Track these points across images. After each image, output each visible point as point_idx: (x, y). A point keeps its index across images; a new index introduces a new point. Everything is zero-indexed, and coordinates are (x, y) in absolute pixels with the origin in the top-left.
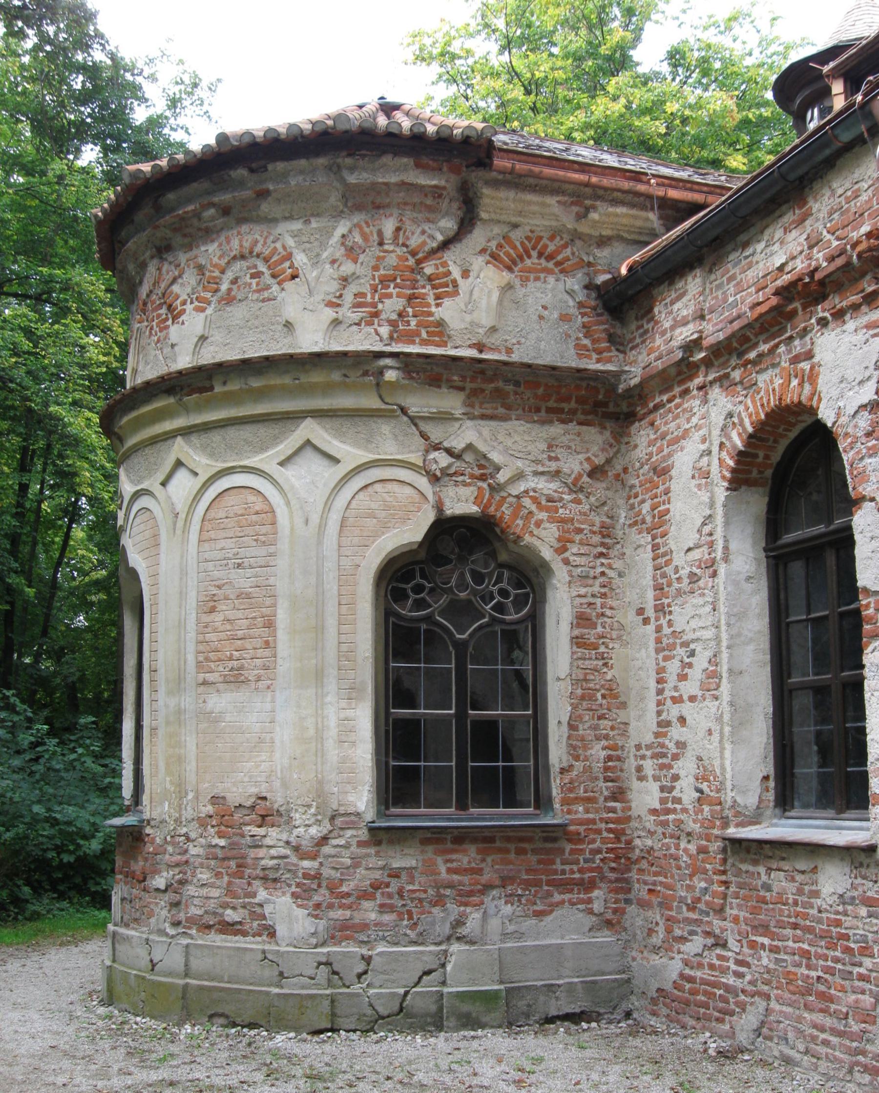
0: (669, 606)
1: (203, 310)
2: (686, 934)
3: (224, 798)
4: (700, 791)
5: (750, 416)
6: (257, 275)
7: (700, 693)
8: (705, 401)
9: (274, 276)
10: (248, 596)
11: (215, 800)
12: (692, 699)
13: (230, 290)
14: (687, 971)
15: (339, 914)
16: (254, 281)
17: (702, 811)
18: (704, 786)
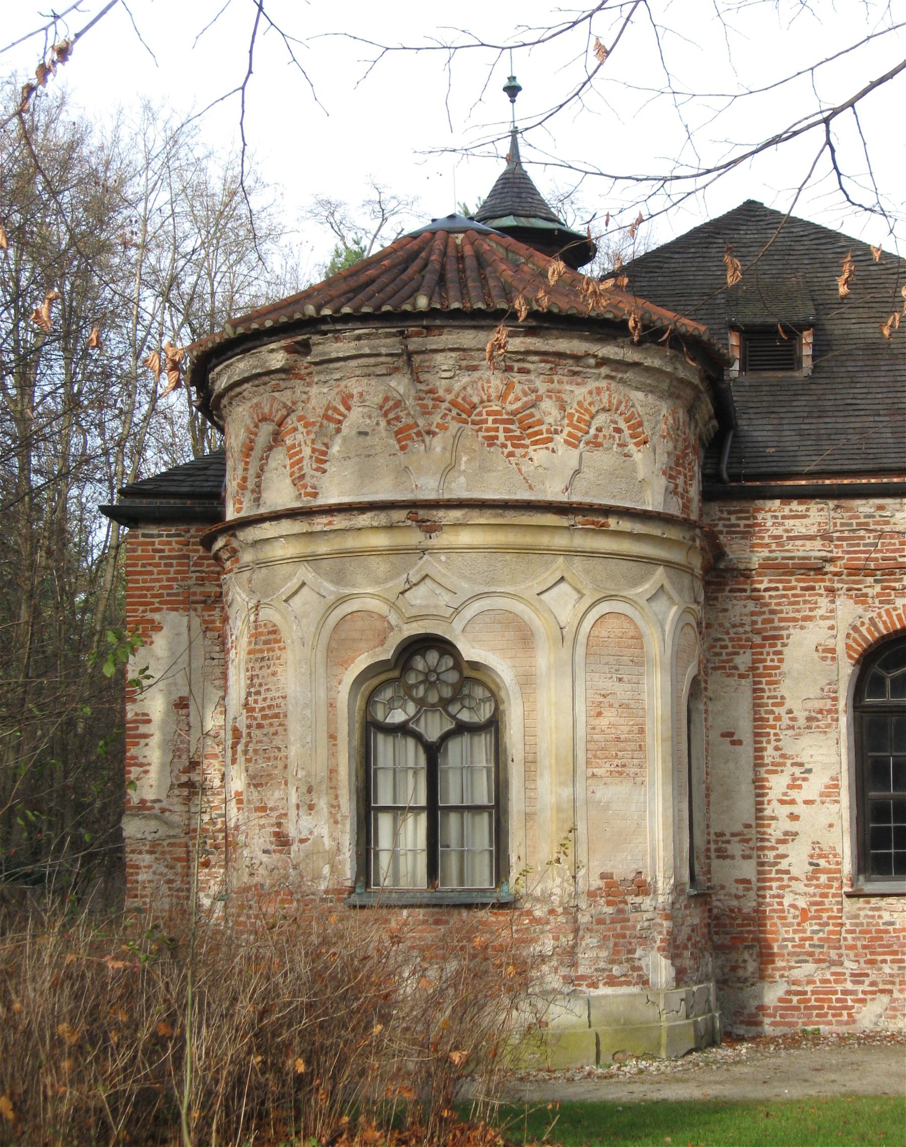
0: (775, 734)
1: (575, 446)
2: (793, 964)
3: (612, 874)
4: (817, 865)
5: (884, 623)
6: (618, 430)
7: (818, 799)
8: (833, 602)
9: (633, 436)
10: (628, 707)
11: (603, 876)
12: (806, 802)
13: (596, 436)
14: (794, 988)
15: (678, 962)
16: (617, 435)
17: (818, 879)
18: (822, 862)
